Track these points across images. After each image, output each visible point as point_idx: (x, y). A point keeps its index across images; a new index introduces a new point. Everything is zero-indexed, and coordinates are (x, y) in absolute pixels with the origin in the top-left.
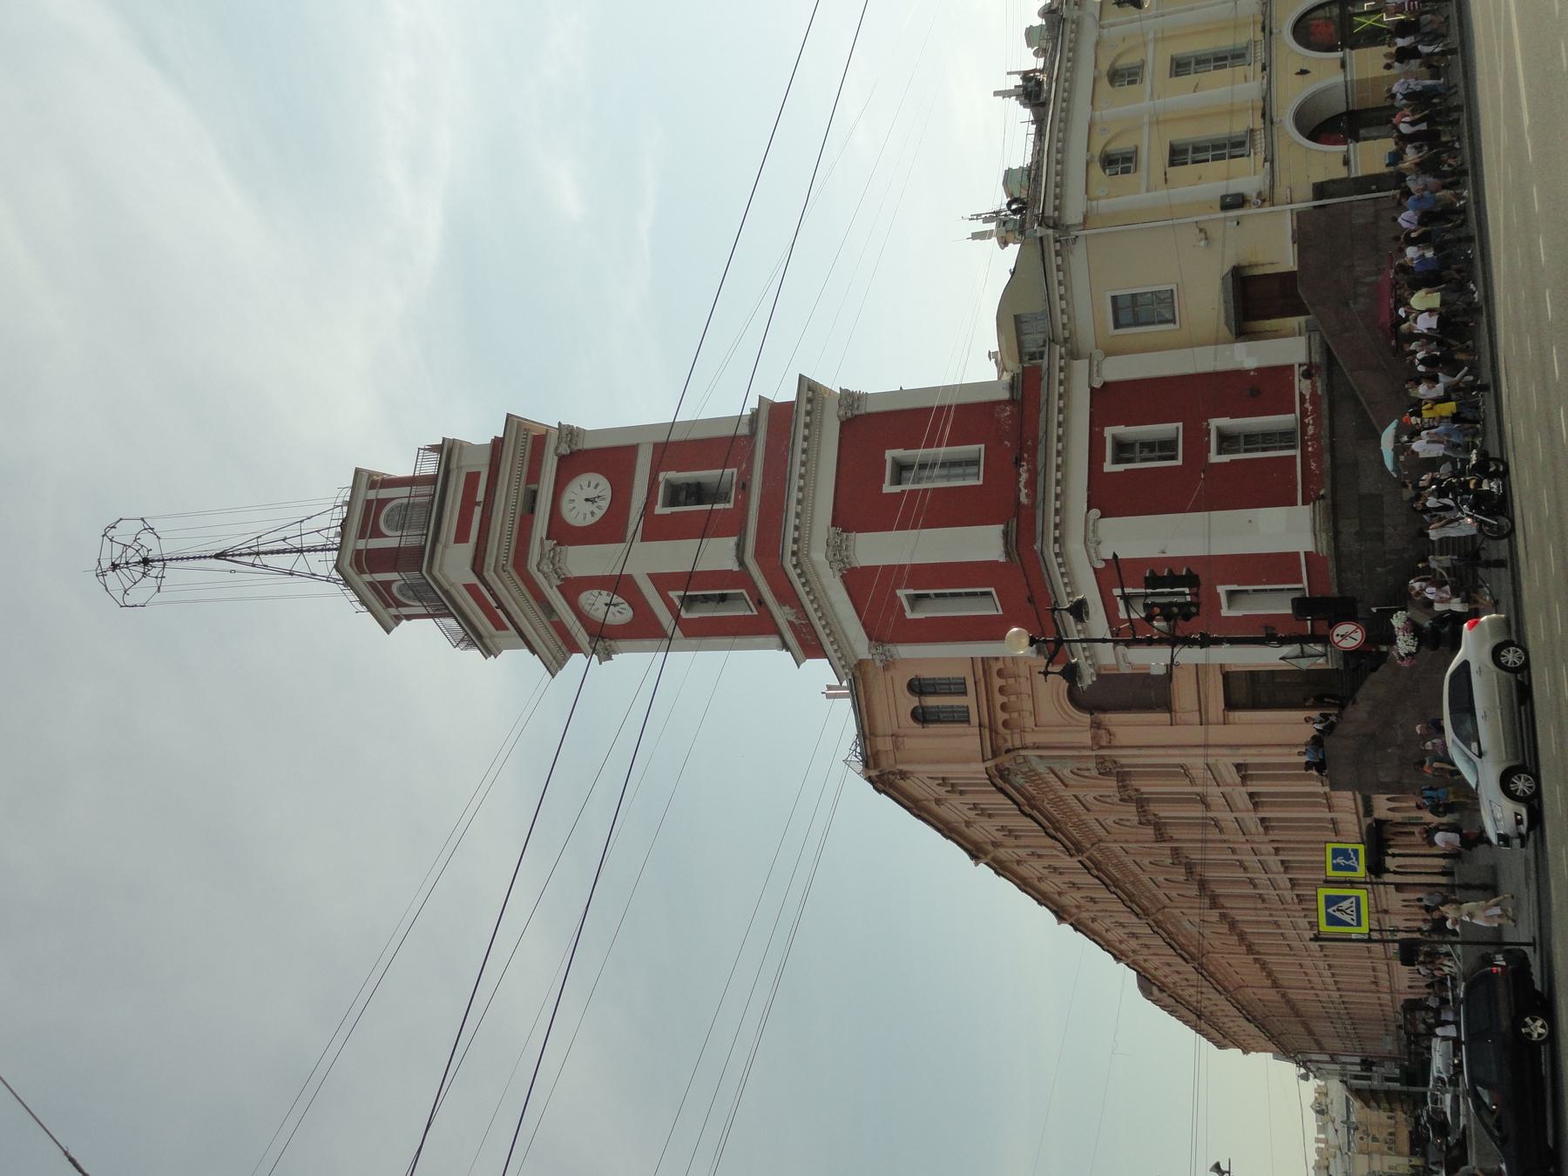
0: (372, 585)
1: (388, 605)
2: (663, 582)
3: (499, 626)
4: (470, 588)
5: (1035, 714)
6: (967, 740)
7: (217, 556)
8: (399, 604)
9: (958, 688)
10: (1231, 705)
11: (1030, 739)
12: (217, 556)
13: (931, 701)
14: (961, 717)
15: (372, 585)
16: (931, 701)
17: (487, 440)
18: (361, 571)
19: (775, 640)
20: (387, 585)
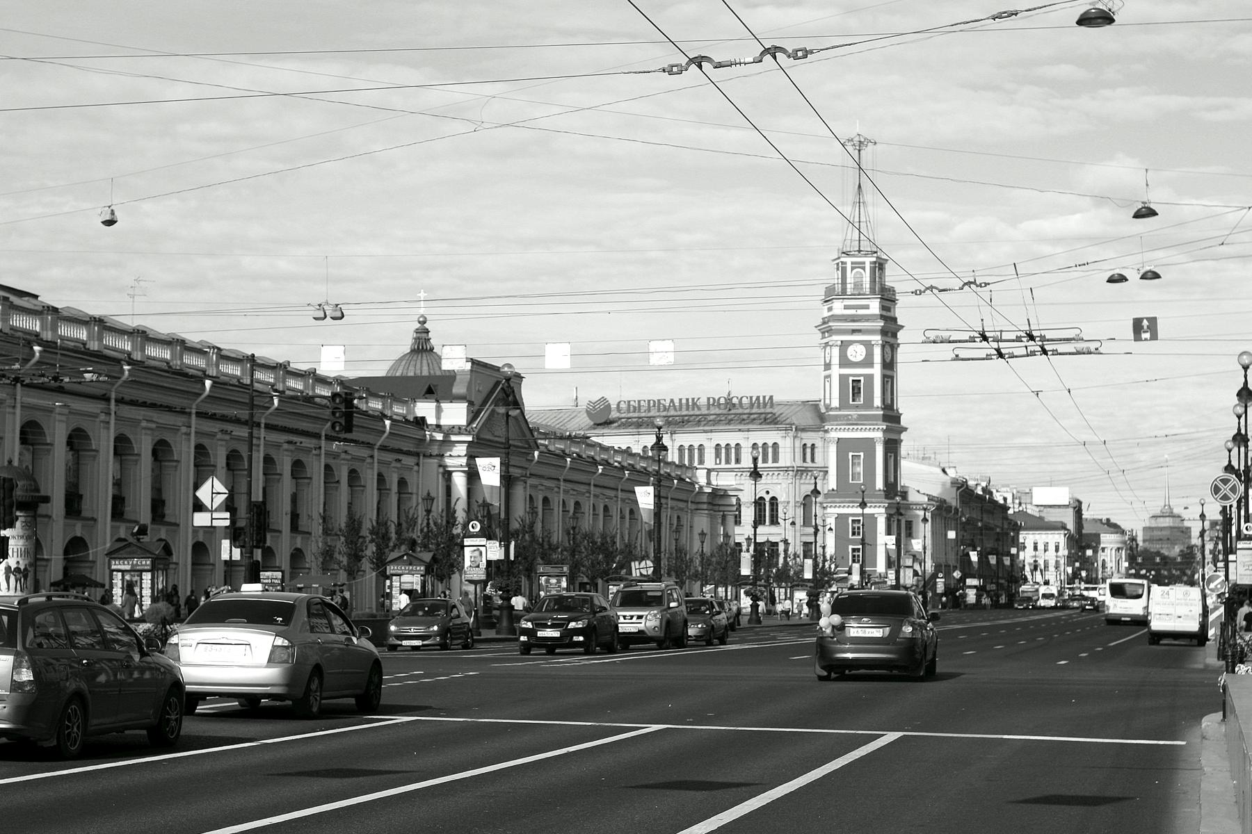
0: (864, 263)
1: (852, 263)
2: (870, 378)
3: (846, 307)
4: (867, 307)
5: (804, 484)
6: (799, 462)
7: (860, 186)
8: (853, 269)
9: (813, 460)
10: (804, 543)
11: (797, 481)
12: (860, 186)
13: (809, 451)
14: (804, 460)
15: (864, 263)
16: (809, 451)
17: (897, 315)
18: (871, 263)
19: (838, 406)
20: (864, 269)
